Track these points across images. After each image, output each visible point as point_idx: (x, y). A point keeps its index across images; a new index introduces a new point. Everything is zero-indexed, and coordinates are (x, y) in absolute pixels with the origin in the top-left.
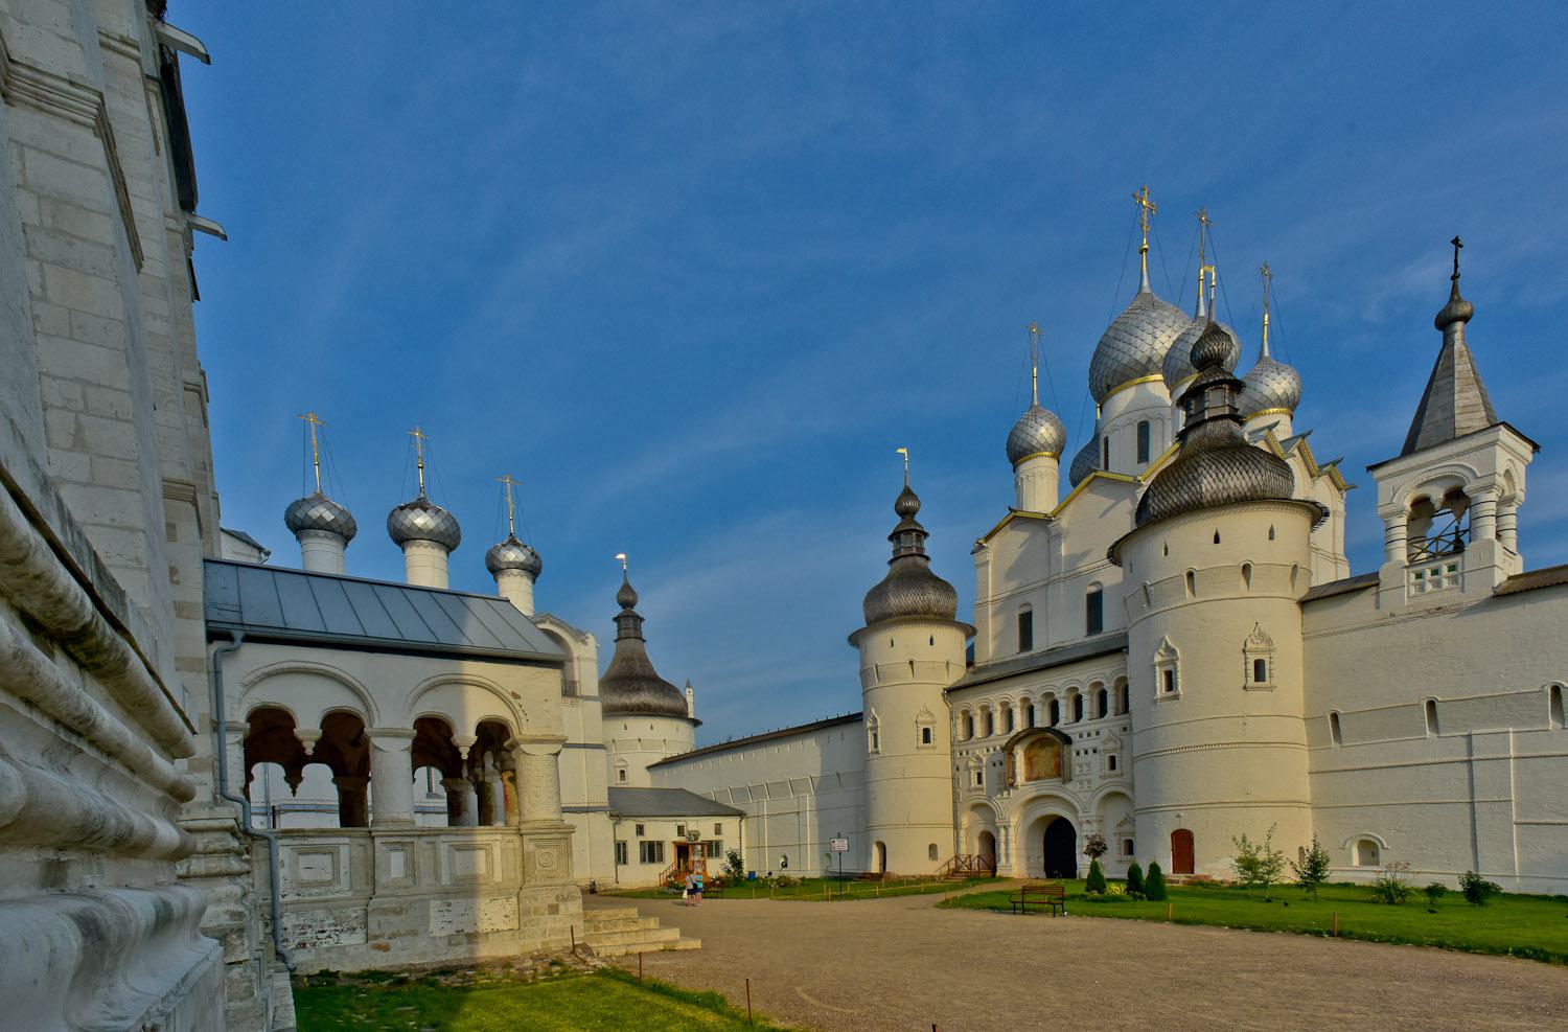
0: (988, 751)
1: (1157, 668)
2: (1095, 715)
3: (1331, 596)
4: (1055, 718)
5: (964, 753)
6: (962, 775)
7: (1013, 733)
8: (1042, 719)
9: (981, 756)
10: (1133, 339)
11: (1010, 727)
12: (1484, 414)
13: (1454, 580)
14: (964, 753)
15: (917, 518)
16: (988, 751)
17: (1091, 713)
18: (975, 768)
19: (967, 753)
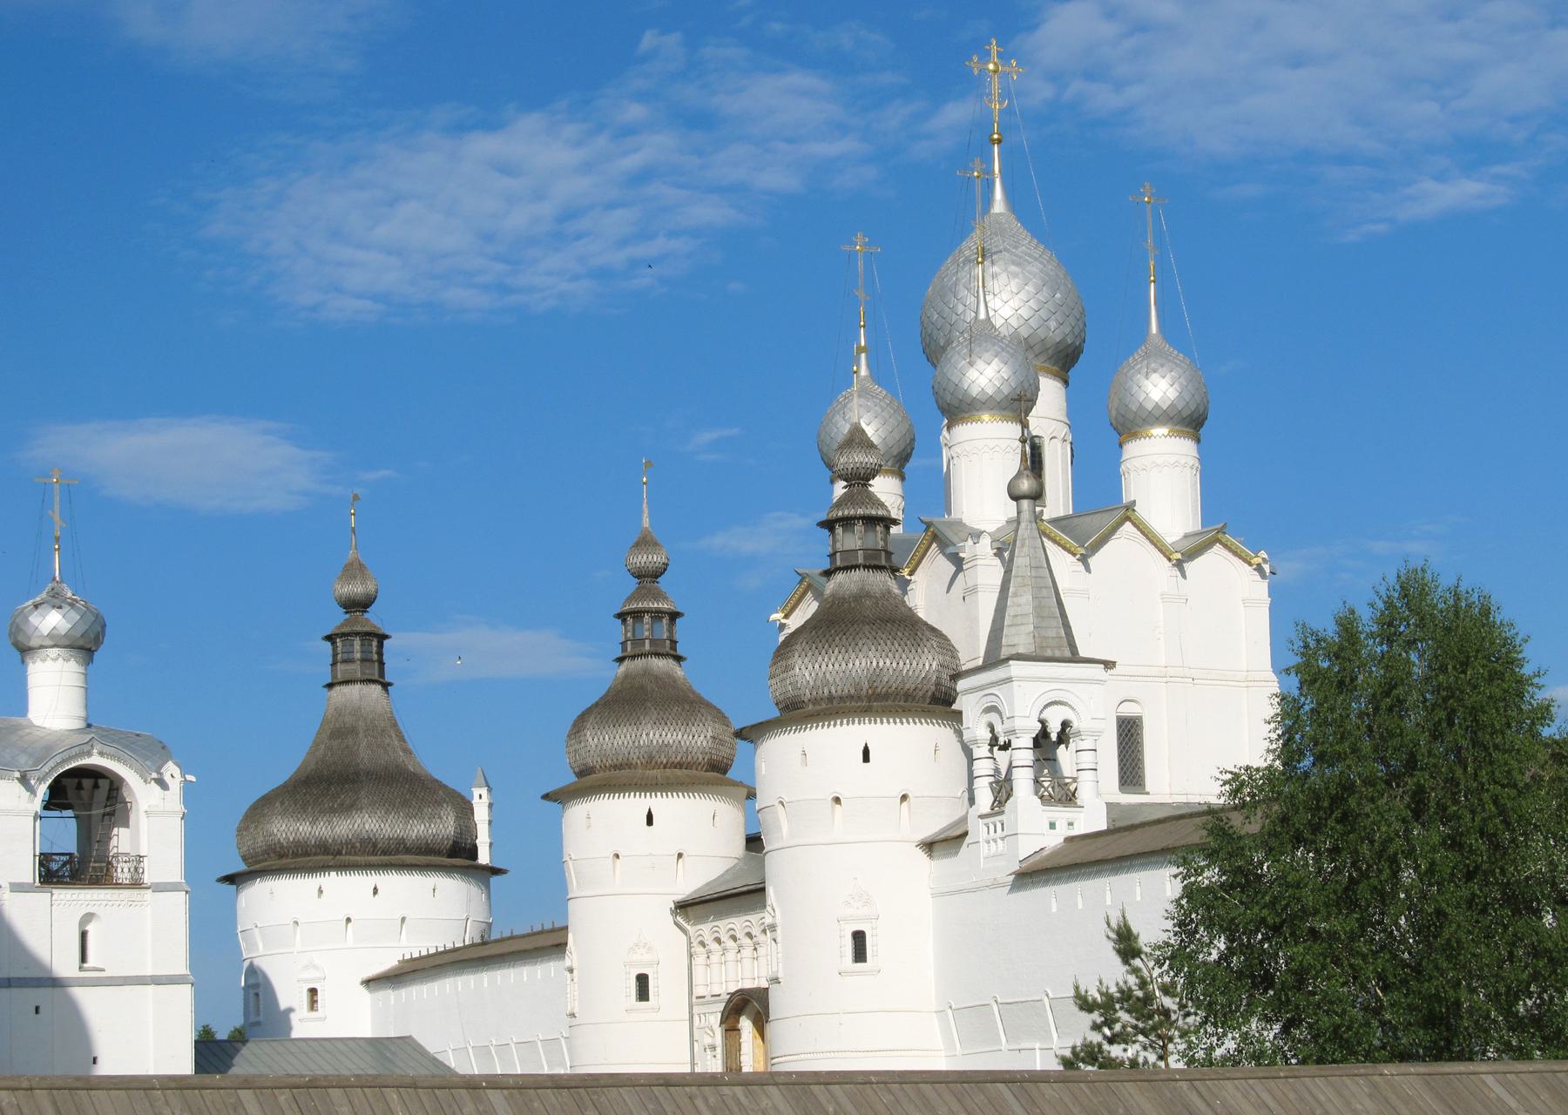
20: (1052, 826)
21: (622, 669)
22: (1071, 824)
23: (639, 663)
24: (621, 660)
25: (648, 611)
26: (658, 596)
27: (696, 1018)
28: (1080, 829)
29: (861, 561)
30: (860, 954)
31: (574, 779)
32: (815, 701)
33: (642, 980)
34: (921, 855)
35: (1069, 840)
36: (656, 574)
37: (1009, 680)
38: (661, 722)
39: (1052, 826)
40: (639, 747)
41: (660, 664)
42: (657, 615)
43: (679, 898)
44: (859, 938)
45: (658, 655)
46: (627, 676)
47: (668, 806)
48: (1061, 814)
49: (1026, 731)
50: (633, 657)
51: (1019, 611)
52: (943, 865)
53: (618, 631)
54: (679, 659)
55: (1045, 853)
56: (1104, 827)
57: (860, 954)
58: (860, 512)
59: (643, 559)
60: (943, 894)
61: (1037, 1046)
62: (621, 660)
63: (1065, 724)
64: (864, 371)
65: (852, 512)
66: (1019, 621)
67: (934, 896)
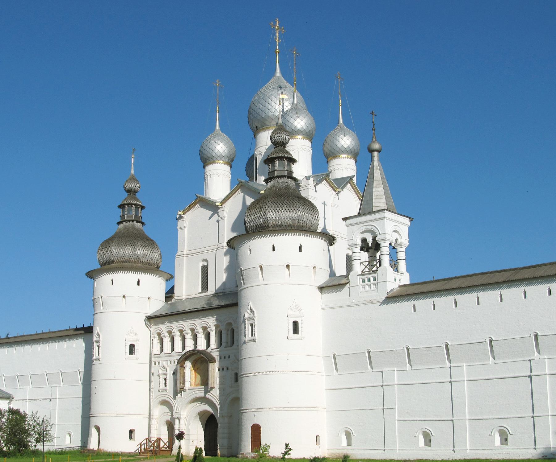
0: (171, 363)
1: (247, 321)
2: (229, 344)
3: (333, 286)
4: (208, 345)
5: (157, 363)
6: (154, 378)
7: (185, 351)
8: (202, 345)
9: (166, 366)
10: (267, 105)
11: (184, 348)
13: (375, 285)
14: (157, 363)
16: (171, 363)
17: (227, 343)
18: (162, 374)
19: (159, 363)
20: (395, 280)
21: (121, 226)
23: (130, 224)
24: (119, 223)
25: (135, 204)
26: (137, 200)
27: (153, 363)
28: (403, 283)
29: (286, 174)
30: (296, 330)
31: (99, 267)
32: (274, 226)
33: (132, 347)
34: (318, 292)
35: (400, 286)
36: (135, 192)
37: (383, 218)
38: (143, 246)
39: (395, 280)
40: (135, 254)
41: (138, 225)
42: (138, 206)
43: (147, 315)
44: (295, 324)
45: (138, 221)
46: (125, 228)
47: (146, 278)
50: (127, 221)
51: (378, 193)
52: (332, 297)
54: (143, 224)
56: (409, 283)
57: (296, 330)
58: (286, 156)
59: (132, 185)
60: (330, 308)
61: (396, 369)
62: (119, 223)
63: (396, 240)
64: (218, 128)
65: (283, 155)
66: (379, 197)
67: (323, 309)
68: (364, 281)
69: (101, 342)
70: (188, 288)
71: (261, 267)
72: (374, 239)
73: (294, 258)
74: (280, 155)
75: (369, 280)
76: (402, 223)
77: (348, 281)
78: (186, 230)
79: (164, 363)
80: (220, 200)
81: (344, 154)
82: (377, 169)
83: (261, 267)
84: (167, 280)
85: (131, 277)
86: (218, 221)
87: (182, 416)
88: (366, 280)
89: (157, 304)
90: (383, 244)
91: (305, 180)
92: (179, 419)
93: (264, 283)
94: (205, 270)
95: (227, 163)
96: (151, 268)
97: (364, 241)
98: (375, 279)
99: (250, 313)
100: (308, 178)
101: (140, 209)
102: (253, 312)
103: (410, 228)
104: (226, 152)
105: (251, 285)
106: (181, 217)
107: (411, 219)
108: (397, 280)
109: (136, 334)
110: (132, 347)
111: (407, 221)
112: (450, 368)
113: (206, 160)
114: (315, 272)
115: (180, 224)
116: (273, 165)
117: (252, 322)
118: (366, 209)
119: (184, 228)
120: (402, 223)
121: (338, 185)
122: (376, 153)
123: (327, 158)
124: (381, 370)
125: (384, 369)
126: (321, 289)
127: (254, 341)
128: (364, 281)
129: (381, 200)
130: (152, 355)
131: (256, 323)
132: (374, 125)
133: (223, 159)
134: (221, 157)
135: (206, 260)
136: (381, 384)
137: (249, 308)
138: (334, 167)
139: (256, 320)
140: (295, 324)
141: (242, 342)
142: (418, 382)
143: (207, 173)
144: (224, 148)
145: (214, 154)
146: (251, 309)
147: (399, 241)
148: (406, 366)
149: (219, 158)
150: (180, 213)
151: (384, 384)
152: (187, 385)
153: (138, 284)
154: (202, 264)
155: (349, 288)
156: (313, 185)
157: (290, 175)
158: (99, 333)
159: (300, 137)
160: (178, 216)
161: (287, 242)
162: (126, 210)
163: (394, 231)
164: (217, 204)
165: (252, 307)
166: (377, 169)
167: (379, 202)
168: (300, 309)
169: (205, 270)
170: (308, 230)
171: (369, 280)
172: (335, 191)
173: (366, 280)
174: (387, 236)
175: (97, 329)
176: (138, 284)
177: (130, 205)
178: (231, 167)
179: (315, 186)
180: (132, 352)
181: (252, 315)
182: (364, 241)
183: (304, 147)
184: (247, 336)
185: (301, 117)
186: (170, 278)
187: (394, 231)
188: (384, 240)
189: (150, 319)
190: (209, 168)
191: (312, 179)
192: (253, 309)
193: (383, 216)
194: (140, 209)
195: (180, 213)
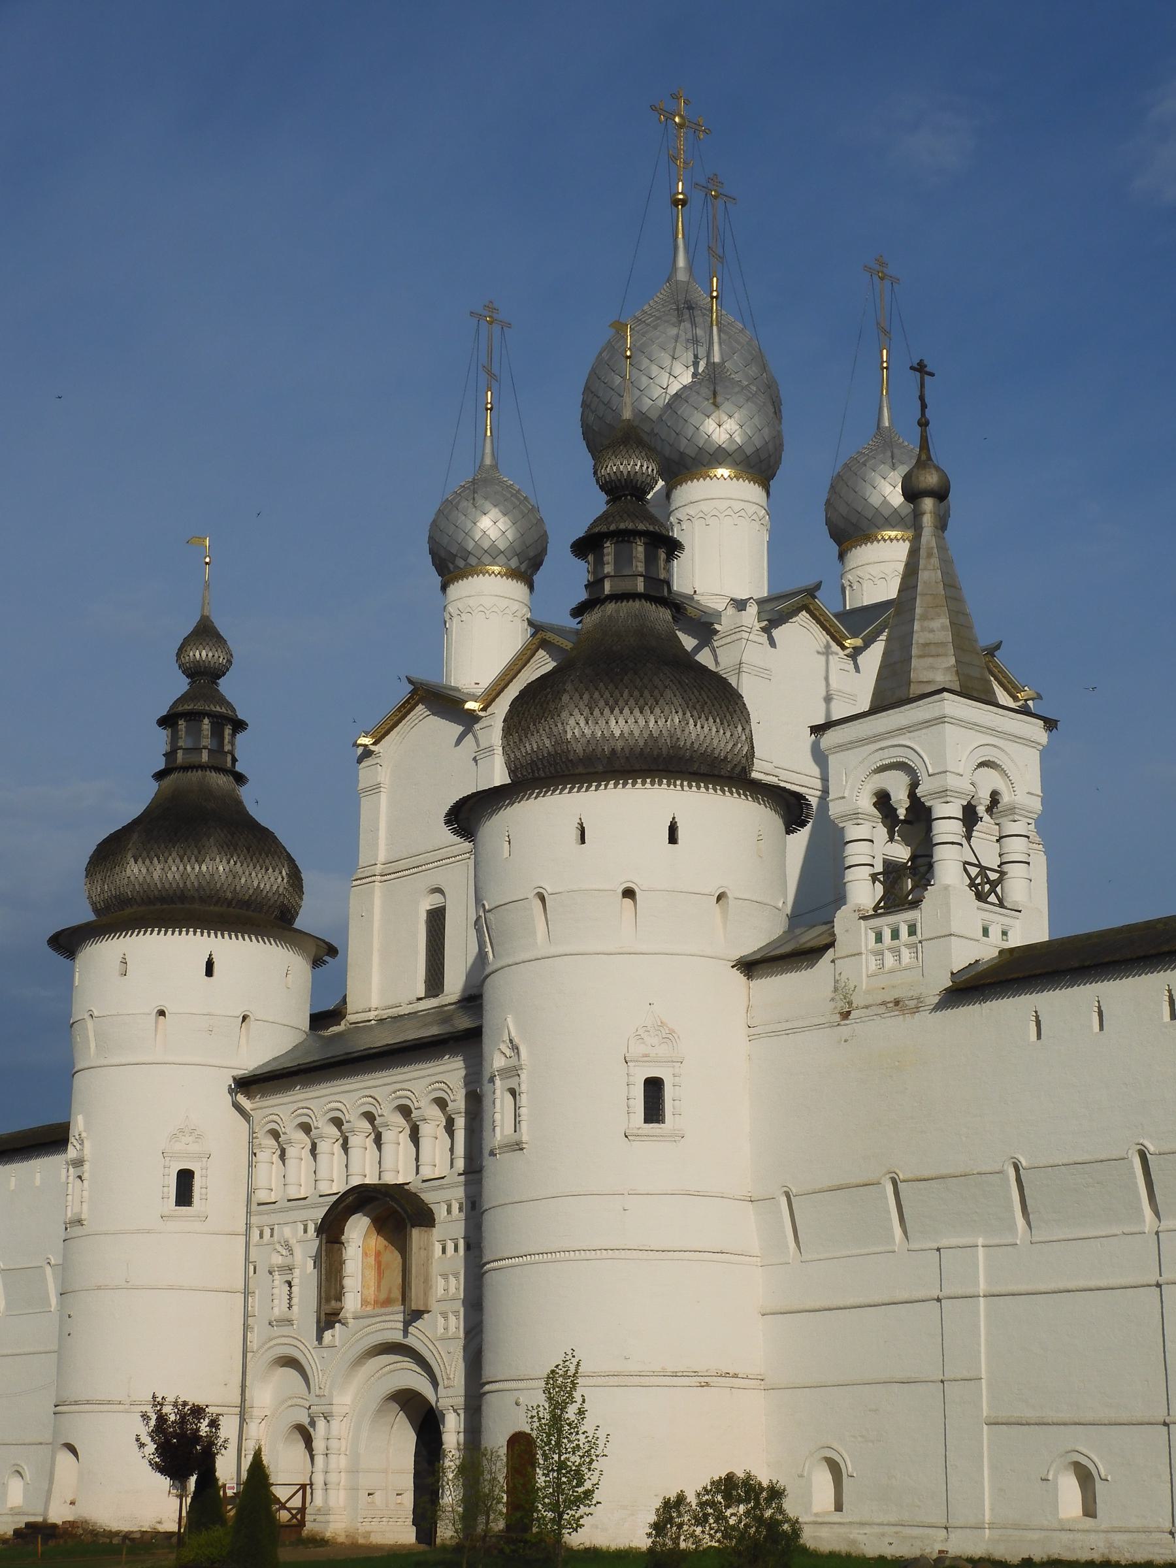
6: (260, 1282)
9: (293, 1242)
12: (952, 661)
15: (225, 686)
20: (986, 932)
22: (1004, 933)
23: (194, 776)
24: (159, 776)
25: (209, 715)
27: (255, 1233)
28: (1016, 940)
30: (654, 1109)
33: (185, 1179)
34: (738, 977)
37: (941, 720)
38: (229, 848)
39: (986, 932)
41: (221, 781)
43: (240, 1073)
44: (654, 1087)
48: (997, 920)
49: (959, 794)
50: (186, 768)
51: (931, 637)
53: (162, 737)
55: (980, 968)
57: (654, 1109)
61: (980, 1241)
63: (995, 797)
65: (631, 526)
68: (879, 938)
69: (87, 1166)
70: (384, 983)
71: (542, 899)
72: (912, 795)
73: (652, 864)
74: (622, 526)
75: (895, 935)
76: (1028, 742)
77: (825, 940)
78: (384, 798)
79: (287, 1232)
80: (479, 691)
81: (893, 527)
82: (930, 555)
83: (542, 899)
84: (317, 962)
85: (184, 948)
86: (475, 759)
87: (335, 1409)
88: (887, 934)
89: (277, 1036)
90: (939, 810)
91: (731, 611)
92: (327, 1417)
93: (553, 950)
94: (436, 919)
95: (514, 574)
96: (270, 919)
97: (883, 801)
98: (912, 931)
99: (508, 1052)
100: (740, 605)
101: (228, 731)
102: (515, 1048)
103: (1046, 755)
104: (510, 535)
105: (517, 960)
106: (367, 753)
107: (1050, 724)
108: (995, 932)
109: (199, 1137)
110: (185, 1179)
111: (1035, 730)
112: (1157, 1233)
113: (451, 563)
114: (725, 913)
115: (366, 774)
116: (599, 562)
117: (512, 1083)
118: (893, 692)
119: (376, 788)
120: (1028, 742)
121: (851, 625)
122: (928, 504)
123: (839, 543)
124: (935, 1246)
125: (944, 1242)
126: (750, 967)
127: (518, 1146)
128: (879, 938)
129: (940, 659)
130: (254, 1207)
131: (524, 1087)
132: (924, 406)
133: (501, 559)
134: (494, 554)
135: (439, 890)
136: (936, 1293)
137: (506, 1038)
138: (859, 572)
139: (523, 1077)
140: (654, 1087)
141: (486, 1152)
142: (1052, 1286)
143: (450, 609)
144: (504, 523)
145: (470, 546)
146: (511, 1041)
147: (1005, 799)
148: (1012, 1227)
149: (486, 559)
150: (367, 741)
151: (947, 1291)
152: (351, 1303)
153: (209, 972)
154: (429, 902)
155: (833, 961)
156: (758, 626)
157: (660, 593)
158: (84, 1135)
159: (723, 472)
160: (360, 750)
161: (627, 815)
162: (182, 733)
163: (982, 764)
164: (470, 705)
165: (513, 1034)
166: (930, 555)
167: (933, 668)
168: (670, 1037)
169: (436, 919)
170: (731, 773)
171: (895, 935)
172: (843, 648)
173: (887, 934)
174: (952, 782)
175: (79, 1125)
176: (209, 972)
177: (194, 717)
178: (531, 587)
179: (766, 630)
180: (184, 1195)
181: (513, 1061)
182: (883, 801)
183: (737, 506)
184: (498, 1129)
185: (727, 406)
186: (324, 953)
187: (982, 764)
188: (943, 794)
189: (247, 1084)
190: (459, 589)
191: (752, 609)
192: (516, 1040)
193: (937, 714)
194: (228, 731)
195: (367, 741)
